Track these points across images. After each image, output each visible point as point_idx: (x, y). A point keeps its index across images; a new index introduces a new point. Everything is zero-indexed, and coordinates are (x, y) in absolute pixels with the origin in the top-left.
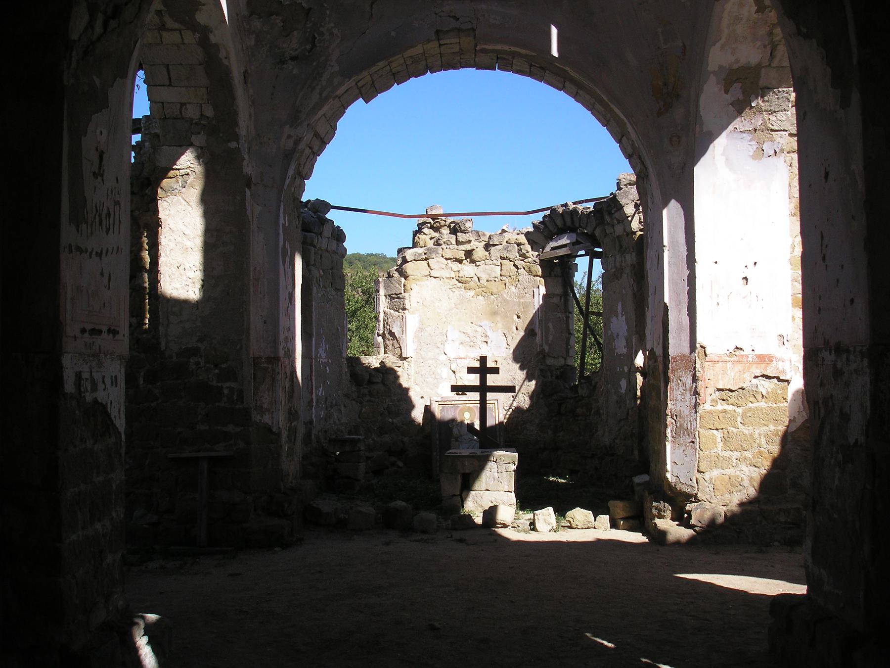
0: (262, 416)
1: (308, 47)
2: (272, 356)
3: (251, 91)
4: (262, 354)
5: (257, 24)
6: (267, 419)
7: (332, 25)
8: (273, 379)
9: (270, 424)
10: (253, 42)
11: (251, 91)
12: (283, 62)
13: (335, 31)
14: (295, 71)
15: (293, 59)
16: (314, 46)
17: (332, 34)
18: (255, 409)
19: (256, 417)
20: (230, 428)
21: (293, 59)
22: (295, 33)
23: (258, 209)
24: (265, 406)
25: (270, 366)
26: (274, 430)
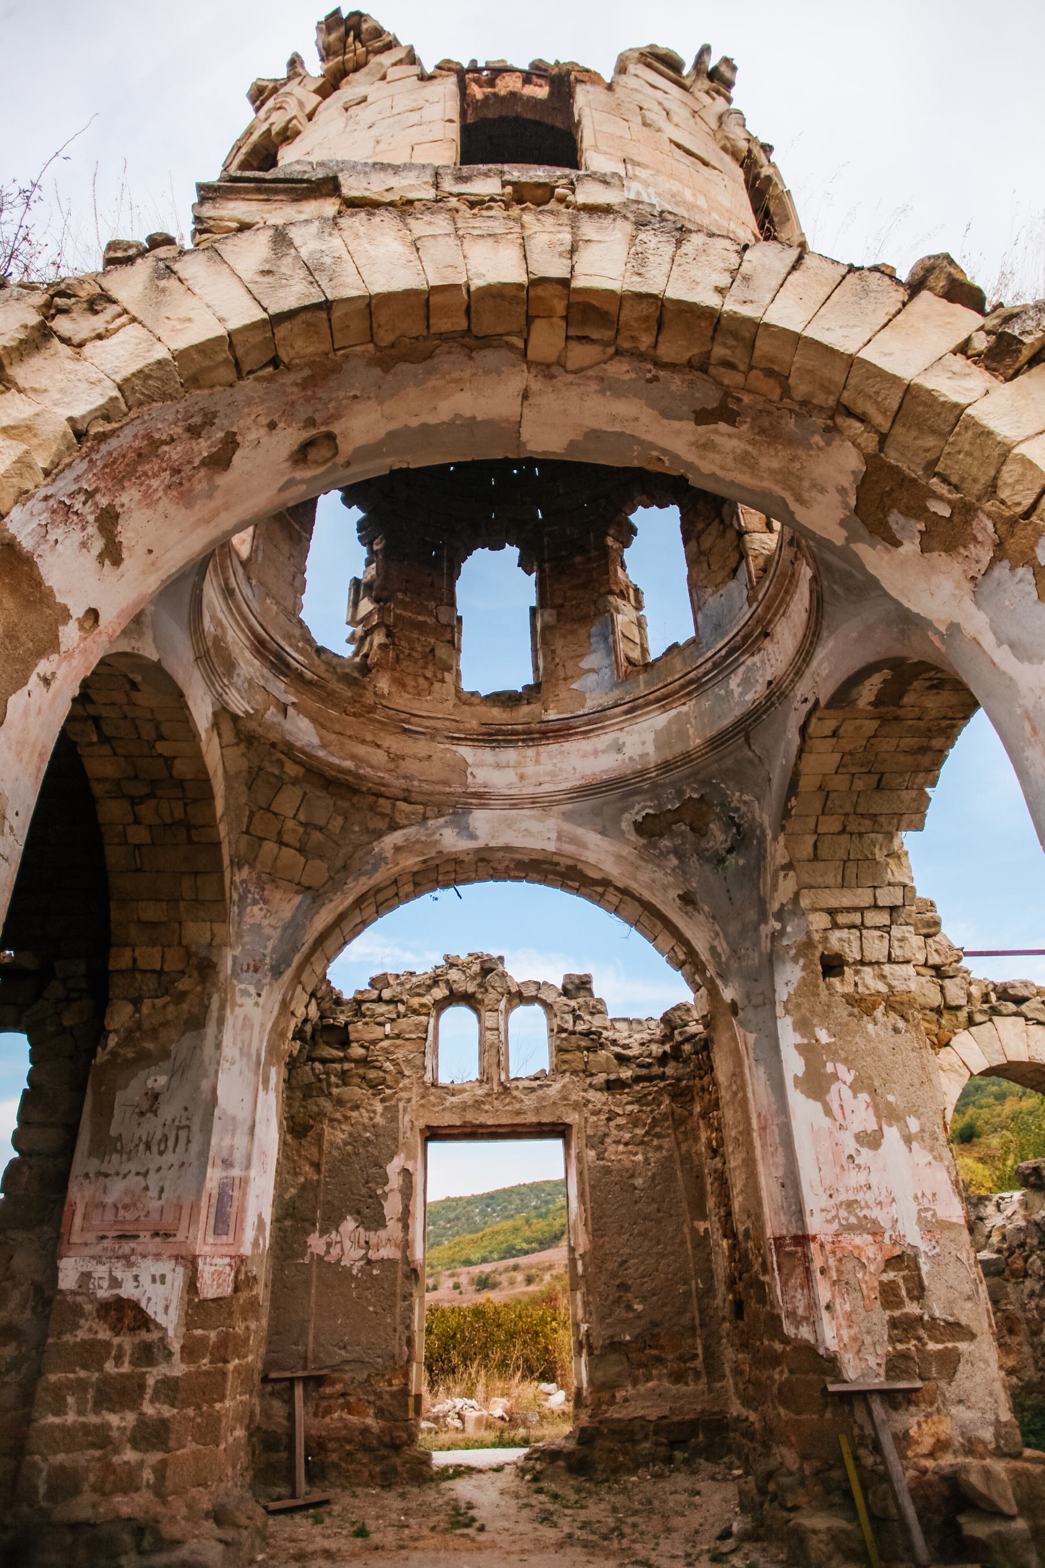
0: (797, 1328)
1: (734, 830)
2: (800, 1233)
3: (706, 908)
4: (784, 1232)
5: (665, 843)
6: (805, 1333)
7: (738, 794)
8: (808, 1271)
9: (813, 1342)
10: (675, 862)
11: (706, 908)
12: (722, 861)
13: (746, 798)
14: (741, 862)
15: (730, 851)
16: (738, 826)
17: (745, 803)
18: (787, 1317)
19: (788, 1328)
20: (778, 1347)
21: (730, 851)
22: (711, 826)
23: (751, 1038)
24: (800, 1312)
25: (799, 1249)
26: (821, 1351)
